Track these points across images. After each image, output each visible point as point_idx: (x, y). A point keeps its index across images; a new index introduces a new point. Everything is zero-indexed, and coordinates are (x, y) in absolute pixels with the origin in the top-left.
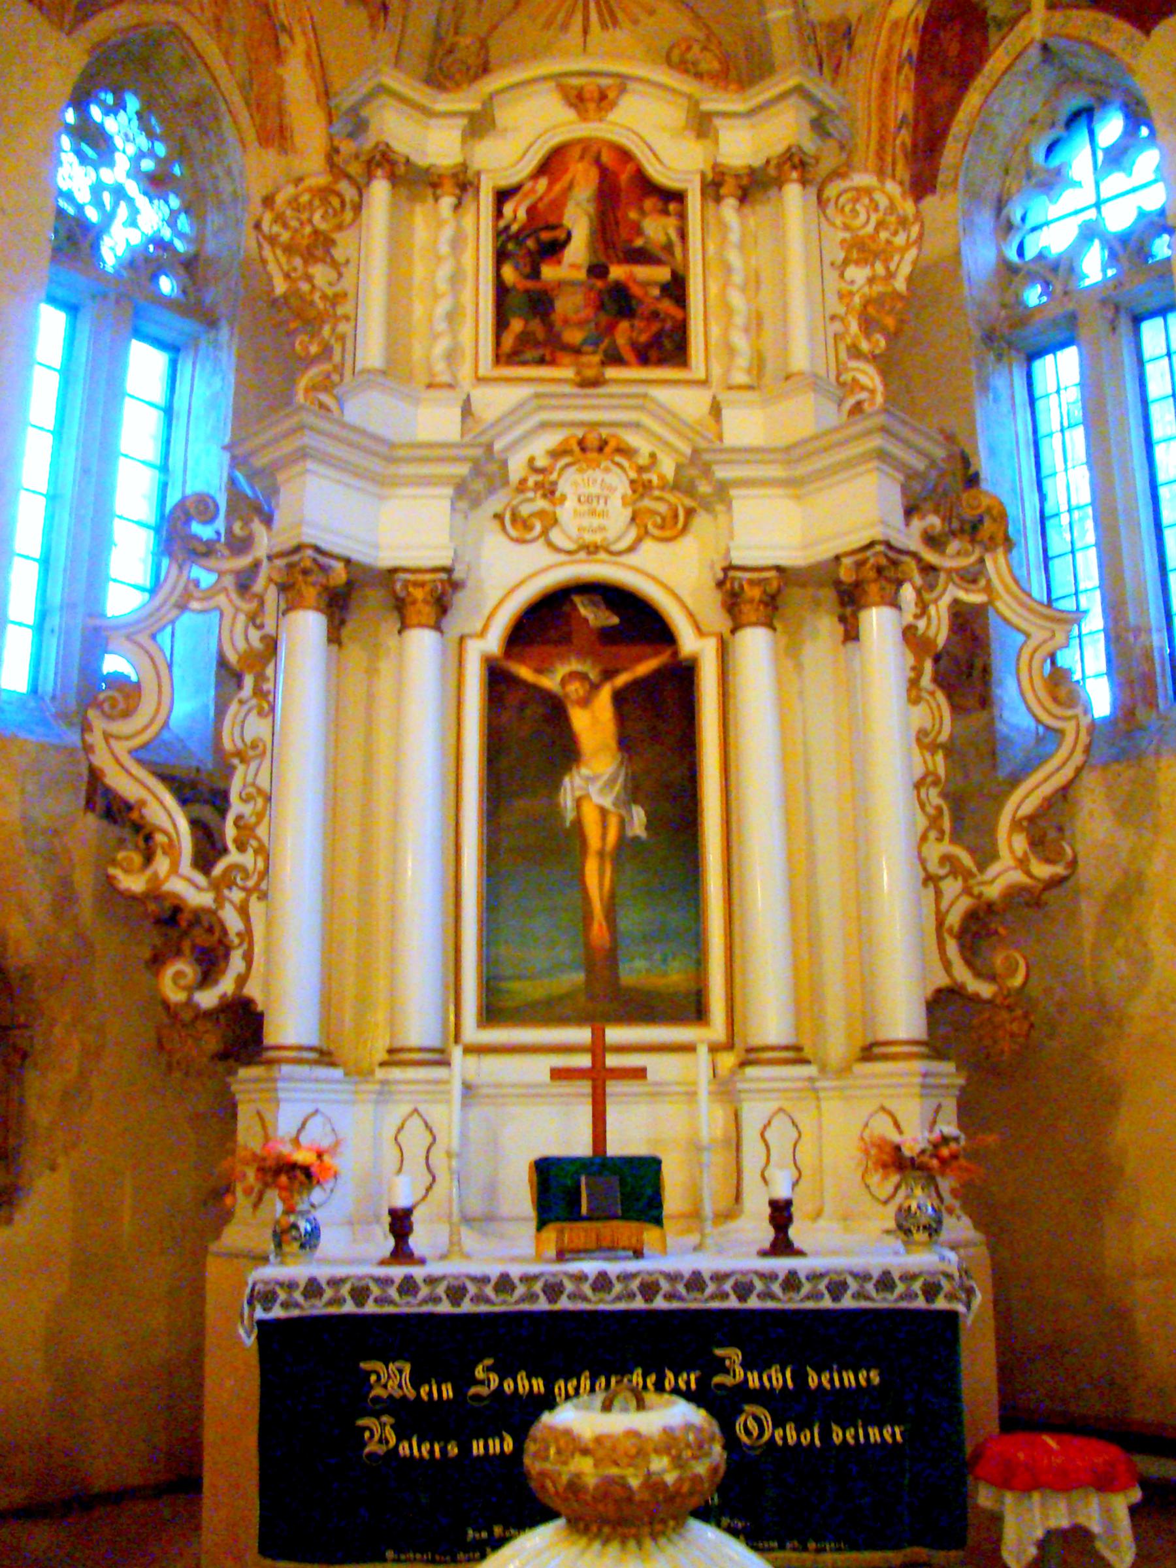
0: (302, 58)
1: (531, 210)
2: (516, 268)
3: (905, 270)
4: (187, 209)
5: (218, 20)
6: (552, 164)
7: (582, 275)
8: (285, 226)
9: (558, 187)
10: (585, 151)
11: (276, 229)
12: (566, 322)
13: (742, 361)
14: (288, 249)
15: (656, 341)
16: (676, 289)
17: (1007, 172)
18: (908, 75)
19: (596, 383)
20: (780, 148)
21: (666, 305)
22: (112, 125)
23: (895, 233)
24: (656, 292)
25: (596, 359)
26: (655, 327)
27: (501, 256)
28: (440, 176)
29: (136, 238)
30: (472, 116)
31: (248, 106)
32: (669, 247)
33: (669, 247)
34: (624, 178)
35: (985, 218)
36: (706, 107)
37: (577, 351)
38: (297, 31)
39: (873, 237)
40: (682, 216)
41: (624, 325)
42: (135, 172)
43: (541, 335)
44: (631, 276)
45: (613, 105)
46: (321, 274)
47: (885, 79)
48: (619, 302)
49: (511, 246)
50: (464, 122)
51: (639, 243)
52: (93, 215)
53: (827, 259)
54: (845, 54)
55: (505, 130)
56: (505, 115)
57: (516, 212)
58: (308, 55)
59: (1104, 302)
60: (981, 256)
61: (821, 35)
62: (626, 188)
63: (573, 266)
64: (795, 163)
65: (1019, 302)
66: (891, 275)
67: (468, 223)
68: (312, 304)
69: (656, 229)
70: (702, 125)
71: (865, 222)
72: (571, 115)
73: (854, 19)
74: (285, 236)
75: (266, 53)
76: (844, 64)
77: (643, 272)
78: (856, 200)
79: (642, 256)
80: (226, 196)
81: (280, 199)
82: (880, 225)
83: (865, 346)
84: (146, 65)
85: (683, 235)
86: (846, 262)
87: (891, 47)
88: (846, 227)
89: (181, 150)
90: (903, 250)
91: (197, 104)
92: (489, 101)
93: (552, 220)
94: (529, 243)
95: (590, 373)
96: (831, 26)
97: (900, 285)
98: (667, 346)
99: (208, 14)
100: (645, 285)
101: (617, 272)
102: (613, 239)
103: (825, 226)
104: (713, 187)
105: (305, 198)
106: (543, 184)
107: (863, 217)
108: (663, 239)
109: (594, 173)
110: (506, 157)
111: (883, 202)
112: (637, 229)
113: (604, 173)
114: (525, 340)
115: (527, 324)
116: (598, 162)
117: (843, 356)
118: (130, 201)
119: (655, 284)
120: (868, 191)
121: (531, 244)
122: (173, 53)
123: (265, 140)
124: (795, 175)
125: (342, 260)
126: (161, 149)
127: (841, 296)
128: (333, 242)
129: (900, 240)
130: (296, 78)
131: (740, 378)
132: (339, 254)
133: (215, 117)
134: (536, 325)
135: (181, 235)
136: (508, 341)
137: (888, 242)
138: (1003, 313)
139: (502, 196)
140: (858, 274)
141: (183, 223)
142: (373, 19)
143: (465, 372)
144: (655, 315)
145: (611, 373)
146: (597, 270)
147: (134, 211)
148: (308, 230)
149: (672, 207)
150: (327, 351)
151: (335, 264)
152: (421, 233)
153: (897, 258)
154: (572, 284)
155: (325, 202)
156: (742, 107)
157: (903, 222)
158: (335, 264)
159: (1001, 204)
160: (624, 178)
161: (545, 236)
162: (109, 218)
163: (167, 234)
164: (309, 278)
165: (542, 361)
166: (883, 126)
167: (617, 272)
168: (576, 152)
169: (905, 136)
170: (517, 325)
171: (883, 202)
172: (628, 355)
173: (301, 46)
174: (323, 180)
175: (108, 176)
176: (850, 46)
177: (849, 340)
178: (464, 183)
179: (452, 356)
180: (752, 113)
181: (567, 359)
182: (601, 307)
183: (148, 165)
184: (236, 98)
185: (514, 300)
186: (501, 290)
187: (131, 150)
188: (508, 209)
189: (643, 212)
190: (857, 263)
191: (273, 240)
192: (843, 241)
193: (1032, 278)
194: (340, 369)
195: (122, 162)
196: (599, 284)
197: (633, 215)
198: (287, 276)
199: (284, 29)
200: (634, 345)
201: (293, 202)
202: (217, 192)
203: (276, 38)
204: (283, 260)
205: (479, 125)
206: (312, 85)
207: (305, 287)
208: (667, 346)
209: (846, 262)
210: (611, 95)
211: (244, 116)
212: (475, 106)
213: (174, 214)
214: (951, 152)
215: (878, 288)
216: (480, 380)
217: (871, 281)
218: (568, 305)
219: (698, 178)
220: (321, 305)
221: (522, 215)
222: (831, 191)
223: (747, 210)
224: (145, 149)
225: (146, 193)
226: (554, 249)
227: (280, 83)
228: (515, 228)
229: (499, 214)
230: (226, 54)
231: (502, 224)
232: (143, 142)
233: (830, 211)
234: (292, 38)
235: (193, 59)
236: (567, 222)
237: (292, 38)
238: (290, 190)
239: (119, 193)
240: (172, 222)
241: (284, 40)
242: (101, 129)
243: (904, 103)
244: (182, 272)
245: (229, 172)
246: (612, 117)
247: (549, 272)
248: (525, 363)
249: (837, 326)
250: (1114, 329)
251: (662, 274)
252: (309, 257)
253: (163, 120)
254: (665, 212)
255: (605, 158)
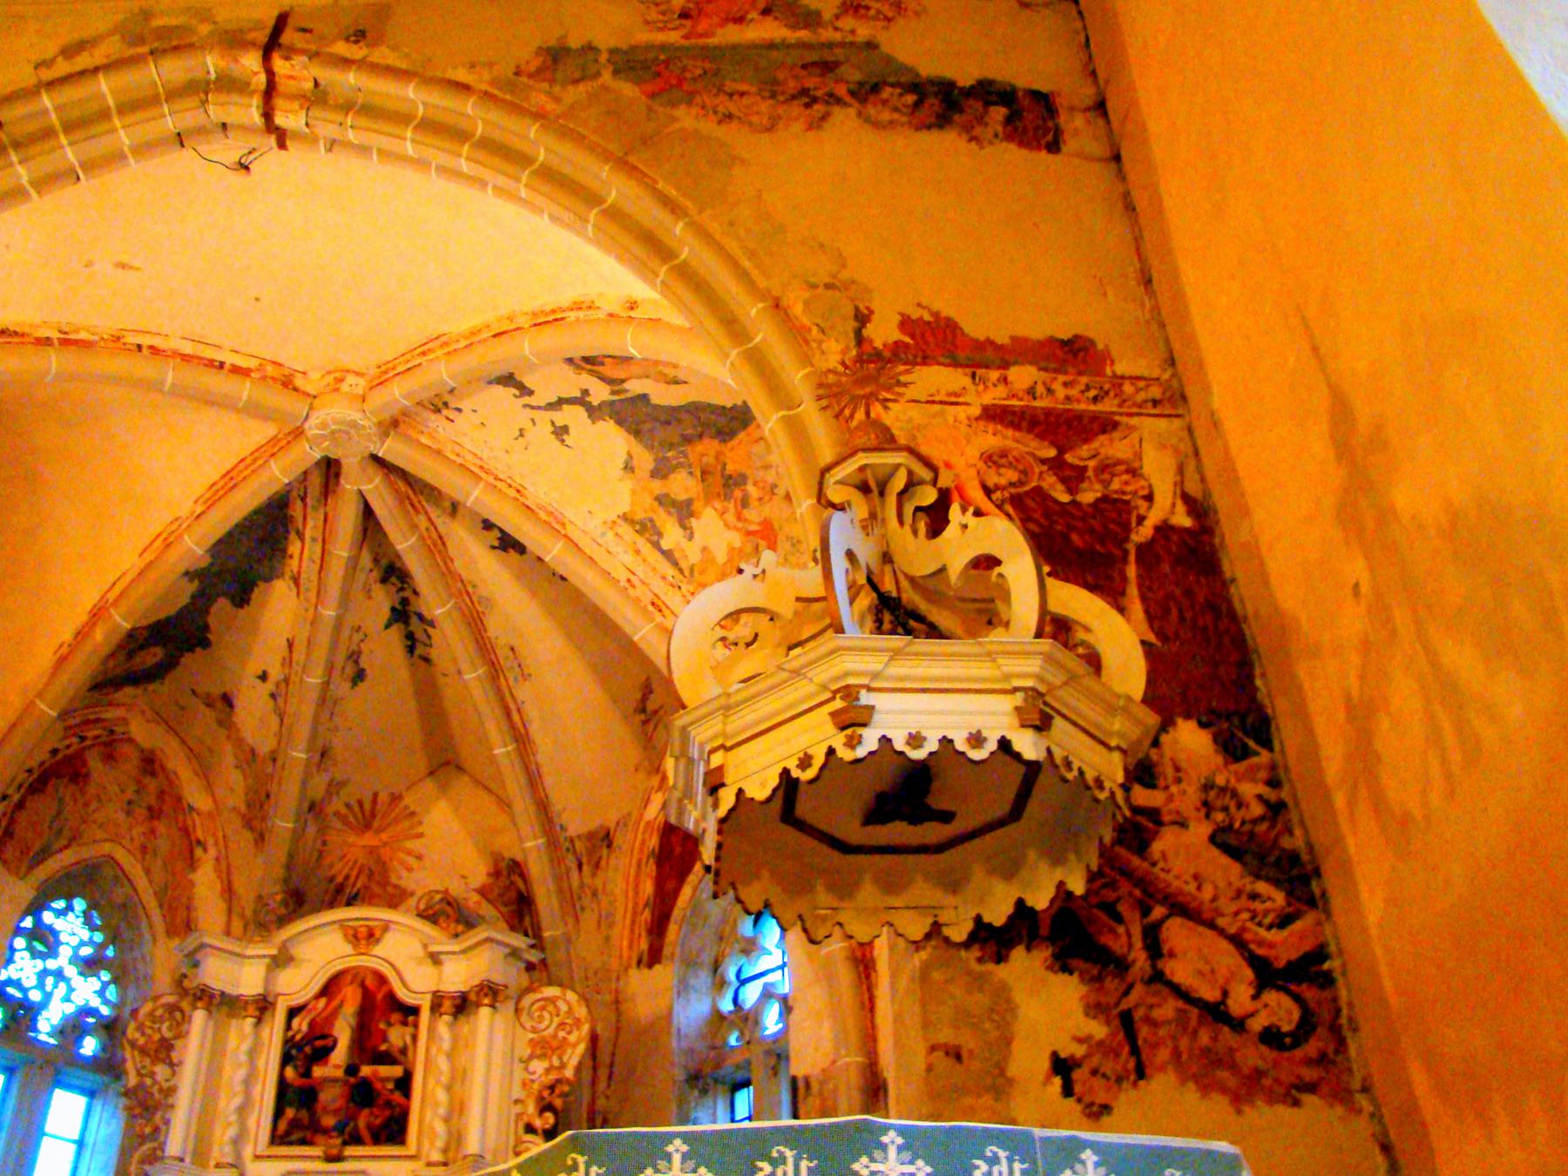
0: (212, 862)
1: (312, 1024)
2: (295, 1067)
3: (574, 1061)
4: (115, 980)
5: (144, 849)
6: (330, 988)
7: (340, 1073)
8: (143, 1034)
9: (335, 1003)
10: (355, 977)
11: (137, 1035)
12: (325, 1110)
13: (440, 1143)
14: (143, 1051)
15: (386, 1124)
16: (404, 1084)
17: (721, 939)
18: (651, 868)
19: (338, 1158)
20: (477, 982)
21: (397, 1096)
22: (59, 924)
23: (569, 1033)
24: (390, 1086)
25: (339, 1141)
26: (387, 1113)
27: (286, 1059)
28: (246, 1002)
29: (70, 1009)
30: (273, 957)
31: (161, 906)
32: (404, 1051)
33: (404, 1051)
34: (379, 997)
35: (703, 979)
36: (434, 948)
37: (326, 1132)
38: (211, 841)
39: (555, 1036)
40: (416, 1026)
41: (366, 1111)
42: (75, 959)
43: (306, 1121)
44: (375, 1074)
45: (378, 941)
46: (161, 1071)
47: (639, 866)
48: (361, 1093)
49: (294, 1052)
50: (267, 960)
51: (383, 1047)
52: (35, 996)
53: (517, 1054)
54: (605, 852)
55: (303, 961)
56: (298, 951)
57: (301, 1024)
58: (217, 859)
59: (768, 1053)
60: (692, 1011)
61: (578, 844)
62: (381, 1005)
63: (337, 1067)
64: (491, 992)
65: (725, 1042)
66: (563, 1066)
67: (265, 1032)
68: (152, 1094)
69: (397, 1036)
70: (435, 959)
71: (549, 1025)
72: (348, 949)
73: (612, 826)
74: (142, 1041)
75: (180, 865)
76: (603, 863)
77: (384, 1070)
78: (543, 1008)
79: (387, 1058)
80: (141, 973)
81: (144, 1011)
82: (562, 1024)
83: (538, 1123)
84: (91, 880)
85: (415, 1038)
86: (531, 1057)
87: (643, 841)
88: (534, 1030)
89: (114, 937)
90: (575, 1045)
91: (124, 906)
92: (284, 947)
93: (326, 1031)
94: (305, 1050)
95: (335, 1152)
96: (591, 836)
97: (569, 1073)
98: (393, 1131)
99: (137, 843)
100: (385, 1080)
101: (366, 1071)
102: (367, 1046)
103: (519, 1030)
104: (437, 1002)
105: (159, 1012)
106: (323, 1001)
107: (547, 1022)
108: (400, 1044)
109: (359, 992)
110: (298, 984)
111: (564, 1008)
112: (384, 1037)
113: (367, 995)
114: (295, 1124)
115: (297, 1115)
116: (363, 985)
117: (521, 1130)
118: (67, 980)
119: (388, 1079)
120: (553, 1000)
121: (308, 1050)
122: (108, 872)
123: (171, 932)
124: (486, 1001)
125: (175, 1061)
126: (99, 937)
127: (524, 1084)
128: (172, 1046)
129: (573, 1038)
130: (205, 882)
131: (436, 1156)
132: (175, 1056)
133: (137, 917)
134: (304, 1114)
135: (106, 1002)
136: (282, 1126)
137: (565, 1039)
138: (713, 1053)
139: (293, 1012)
140: (539, 1066)
141: (112, 993)
142: (256, 841)
143: (248, 1152)
144: (388, 1104)
145: (349, 1151)
146: (352, 1070)
147: (71, 990)
148: (157, 1037)
149: (411, 1018)
150: (156, 1130)
151: (172, 1065)
152: (233, 1041)
153: (569, 1051)
154: (335, 1080)
155: (172, 1018)
156: (456, 948)
157: (578, 1023)
158: (172, 1065)
159: (716, 966)
160: (379, 997)
161: (319, 1043)
162: (48, 996)
163: (95, 1002)
164: (152, 1074)
165: (303, 1142)
166: (636, 904)
167: (366, 1071)
168: (349, 977)
169: (647, 914)
170: (290, 1113)
171: (564, 1008)
172: (366, 1135)
173: (212, 852)
174: (171, 999)
175: (52, 964)
176: (609, 846)
177: (526, 1119)
178: (264, 1005)
179: (237, 1141)
180: (464, 952)
181: (320, 1139)
182: (351, 1098)
183: (87, 951)
184: (152, 904)
185: (290, 1095)
186: (282, 1084)
187: (75, 941)
188: (295, 1022)
189: (390, 1025)
190: (539, 1057)
191: (133, 1044)
192: (531, 1040)
193: (733, 1025)
194: (162, 1147)
195: (65, 952)
196: (352, 1080)
197: (382, 1026)
198: (139, 1074)
199: (199, 842)
200: (369, 1127)
201: (151, 1014)
202: (135, 969)
203: (192, 852)
204: (138, 1059)
205: (282, 960)
206: (218, 881)
207: (148, 1081)
208: (393, 1131)
209: (531, 1057)
210: (378, 934)
211: (157, 918)
212: (274, 952)
213: (105, 985)
214: (672, 928)
215: (552, 1077)
216: (257, 1157)
217: (548, 1071)
218: (330, 1096)
219: (429, 996)
220: (157, 1096)
221: (305, 1027)
222: (527, 1001)
223: (462, 1018)
224: (86, 939)
225: (81, 974)
226: (322, 1055)
227: (192, 884)
228: (298, 1037)
229: (288, 1027)
230: (148, 871)
231: (290, 1034)
232: (85, 934)
233: (524, 1018)
234: (205, 850)
235: (123, 875)
236: (335, 1033)
237: (205, 850)
238: (149, 1006)
239: (59, 975)
240: (101, 993)
241: (198, 852)
242: (51, 929)
243: (648, 888)
244: (102, 1032)
245: (144, 958)
246: (378, 950)
247: (318, 1072)
248: (290, 1143)
249: (519, 1108)
250: (775, 1074)
251: (397, 1071)
252: (156, 1060)
253: (101, 917)
254: (405, 1024)
255: (369, 982)
